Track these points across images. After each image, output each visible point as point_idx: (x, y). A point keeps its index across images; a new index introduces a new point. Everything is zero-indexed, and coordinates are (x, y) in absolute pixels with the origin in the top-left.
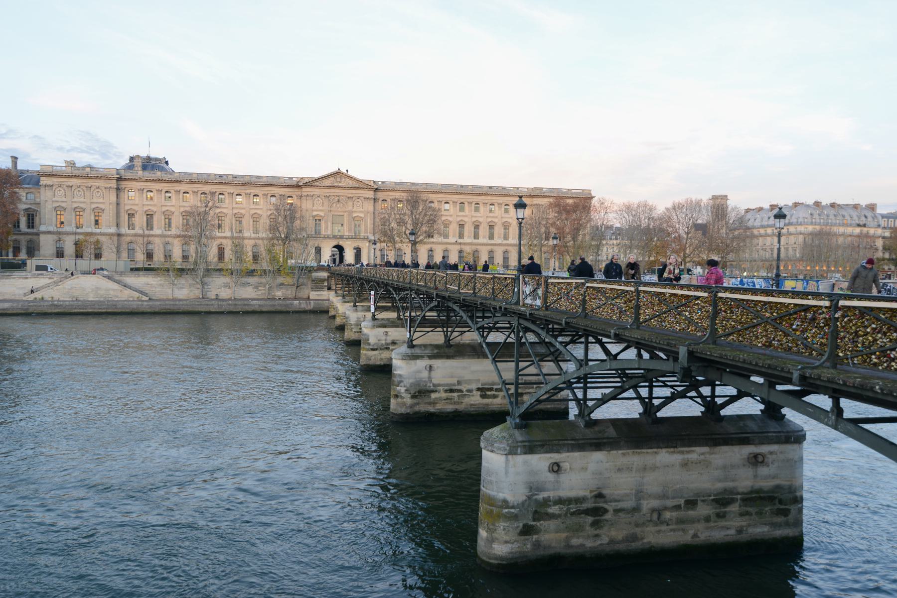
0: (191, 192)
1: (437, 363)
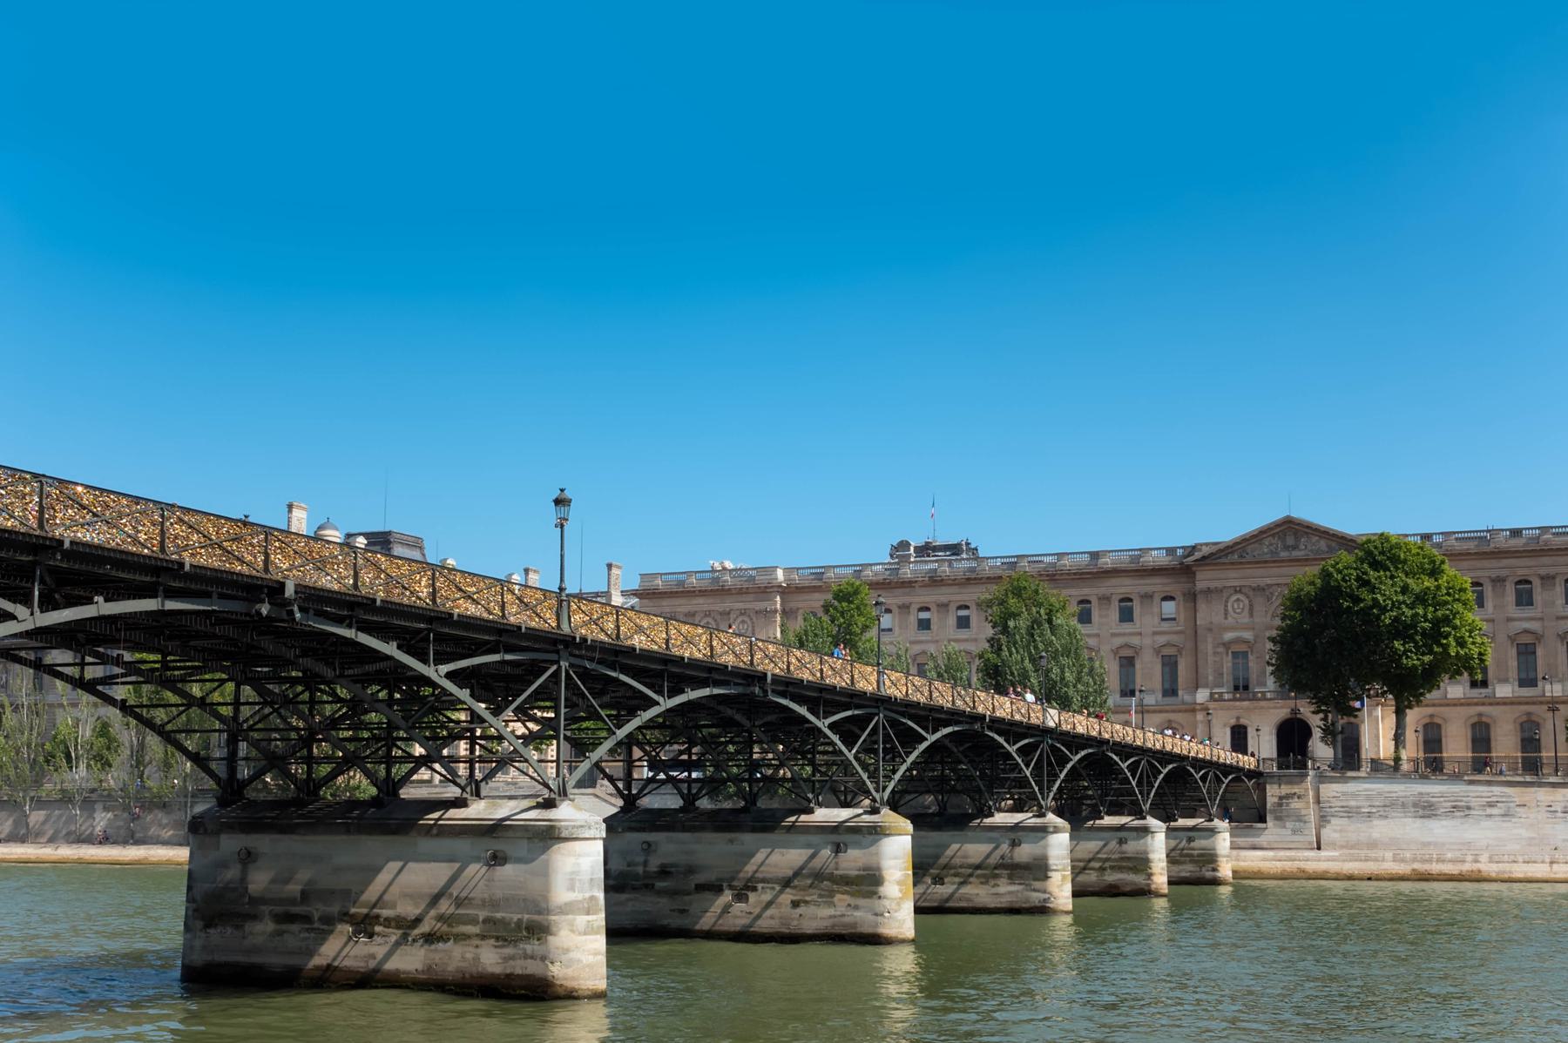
0: (934, 608)
1: (262, 843)
